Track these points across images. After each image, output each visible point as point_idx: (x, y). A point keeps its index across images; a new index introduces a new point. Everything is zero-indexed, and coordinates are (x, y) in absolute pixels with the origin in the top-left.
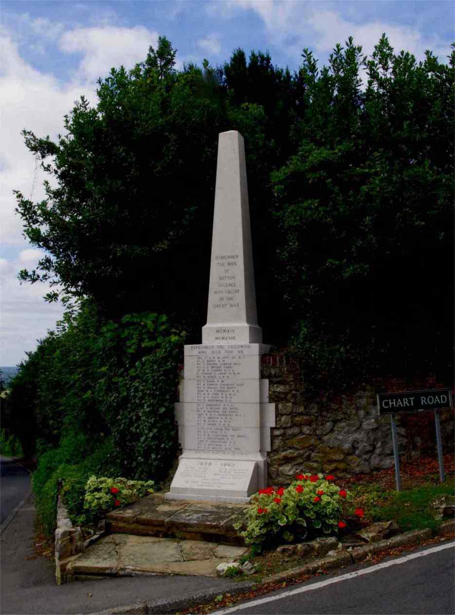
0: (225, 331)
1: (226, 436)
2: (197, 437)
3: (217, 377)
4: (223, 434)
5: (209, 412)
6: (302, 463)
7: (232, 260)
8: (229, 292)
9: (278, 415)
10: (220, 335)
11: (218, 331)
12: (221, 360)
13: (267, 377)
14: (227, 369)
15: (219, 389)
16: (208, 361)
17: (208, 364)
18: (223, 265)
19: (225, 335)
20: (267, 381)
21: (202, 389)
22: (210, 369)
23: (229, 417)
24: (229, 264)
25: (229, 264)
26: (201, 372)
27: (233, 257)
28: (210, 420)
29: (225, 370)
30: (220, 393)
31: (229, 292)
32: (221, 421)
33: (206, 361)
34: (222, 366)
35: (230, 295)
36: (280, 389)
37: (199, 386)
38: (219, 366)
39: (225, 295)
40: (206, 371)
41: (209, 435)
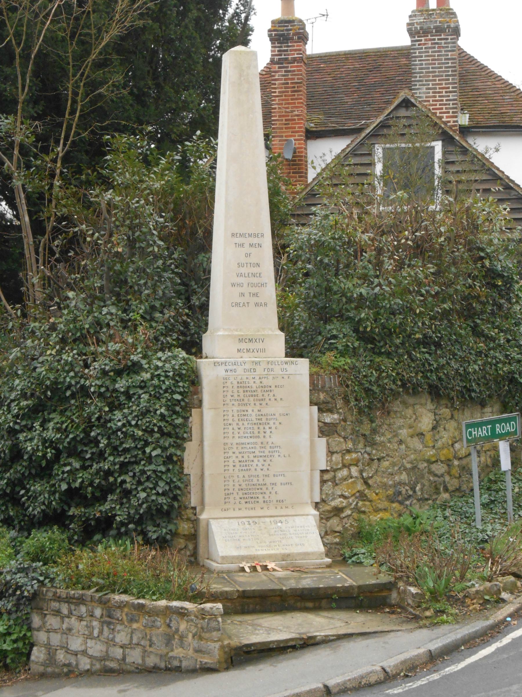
0: (250, 340)
1: (265, 484)
2: (224, 488)
3: (252, 404)
4: (261, 482)
5: (240, 453)
6: (350, 515)
7: (255, 241)
8: (253, 285)
9: (331, 453)
10: (244, 346)
11: (240, 340)
12: (258, 381)
13: (316, 404)
14: (266, 394)
15: (255, 422)
16: (238, 382)
17: (238, 387)
18: (242, 245)
19: (250, 346)
20: (315, 408)
21: (230, 421)
22: (242, 394)
23: (268, 459)
24: (251, 245)
25: (251, 245)
26: (229, 397)
27: (256, 235)
28: (242, 464)
29: (263, 395)
30: (256, 427)
31: (253, 285)
32: (257, 465)
33: (235, 382)
34: (259, 390)
35: (254, 290)
36: (328, 418)
37: (226, 417)
38: (255, 389)
39: (245, 289)
40: (236, 397)
41: (240, 485)
